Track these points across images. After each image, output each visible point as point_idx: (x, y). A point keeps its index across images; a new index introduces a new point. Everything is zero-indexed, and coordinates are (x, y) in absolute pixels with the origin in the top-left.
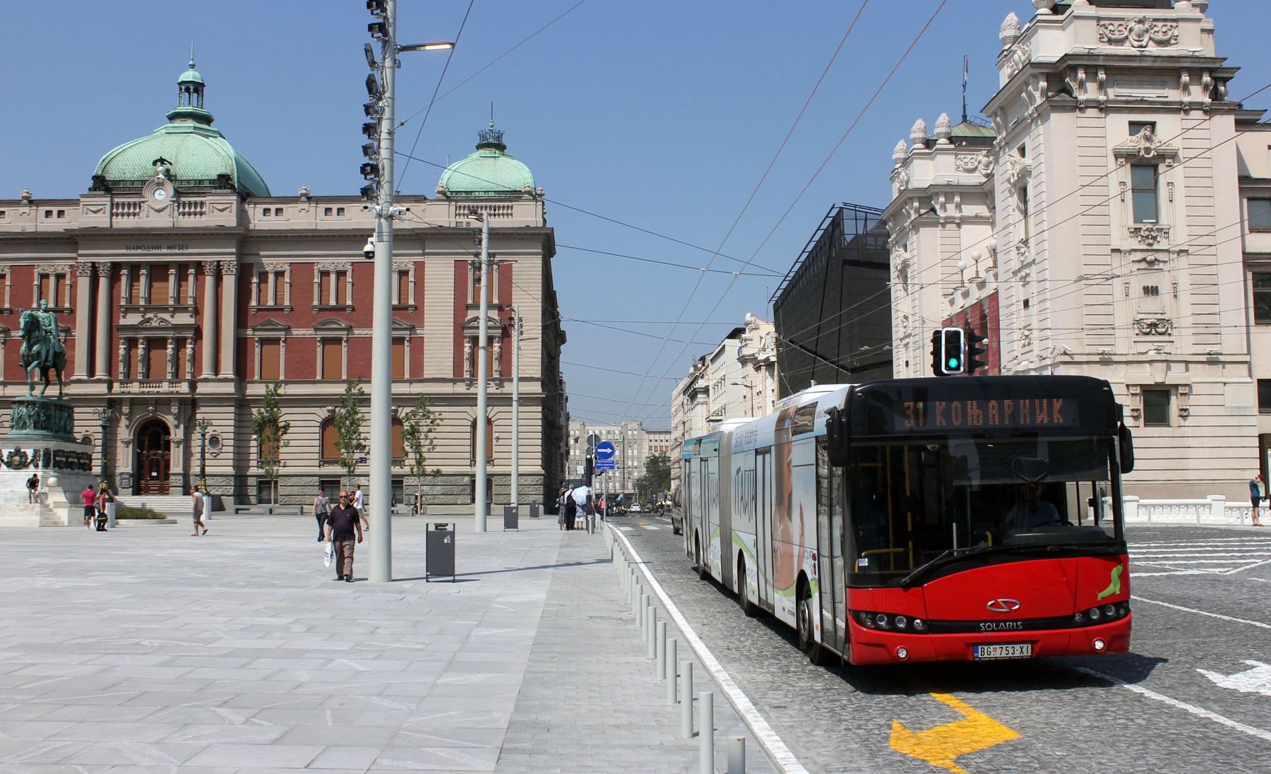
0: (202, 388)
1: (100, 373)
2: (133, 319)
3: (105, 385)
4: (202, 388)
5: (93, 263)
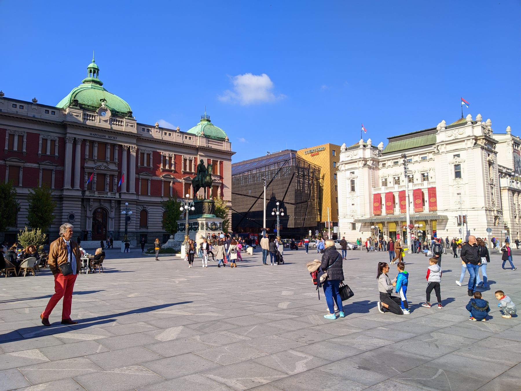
0: (123, 197)
1: (77, 186)
2: (89, 164)
3: (81, 192)
4: (123, 197)
5: (75, 138)
